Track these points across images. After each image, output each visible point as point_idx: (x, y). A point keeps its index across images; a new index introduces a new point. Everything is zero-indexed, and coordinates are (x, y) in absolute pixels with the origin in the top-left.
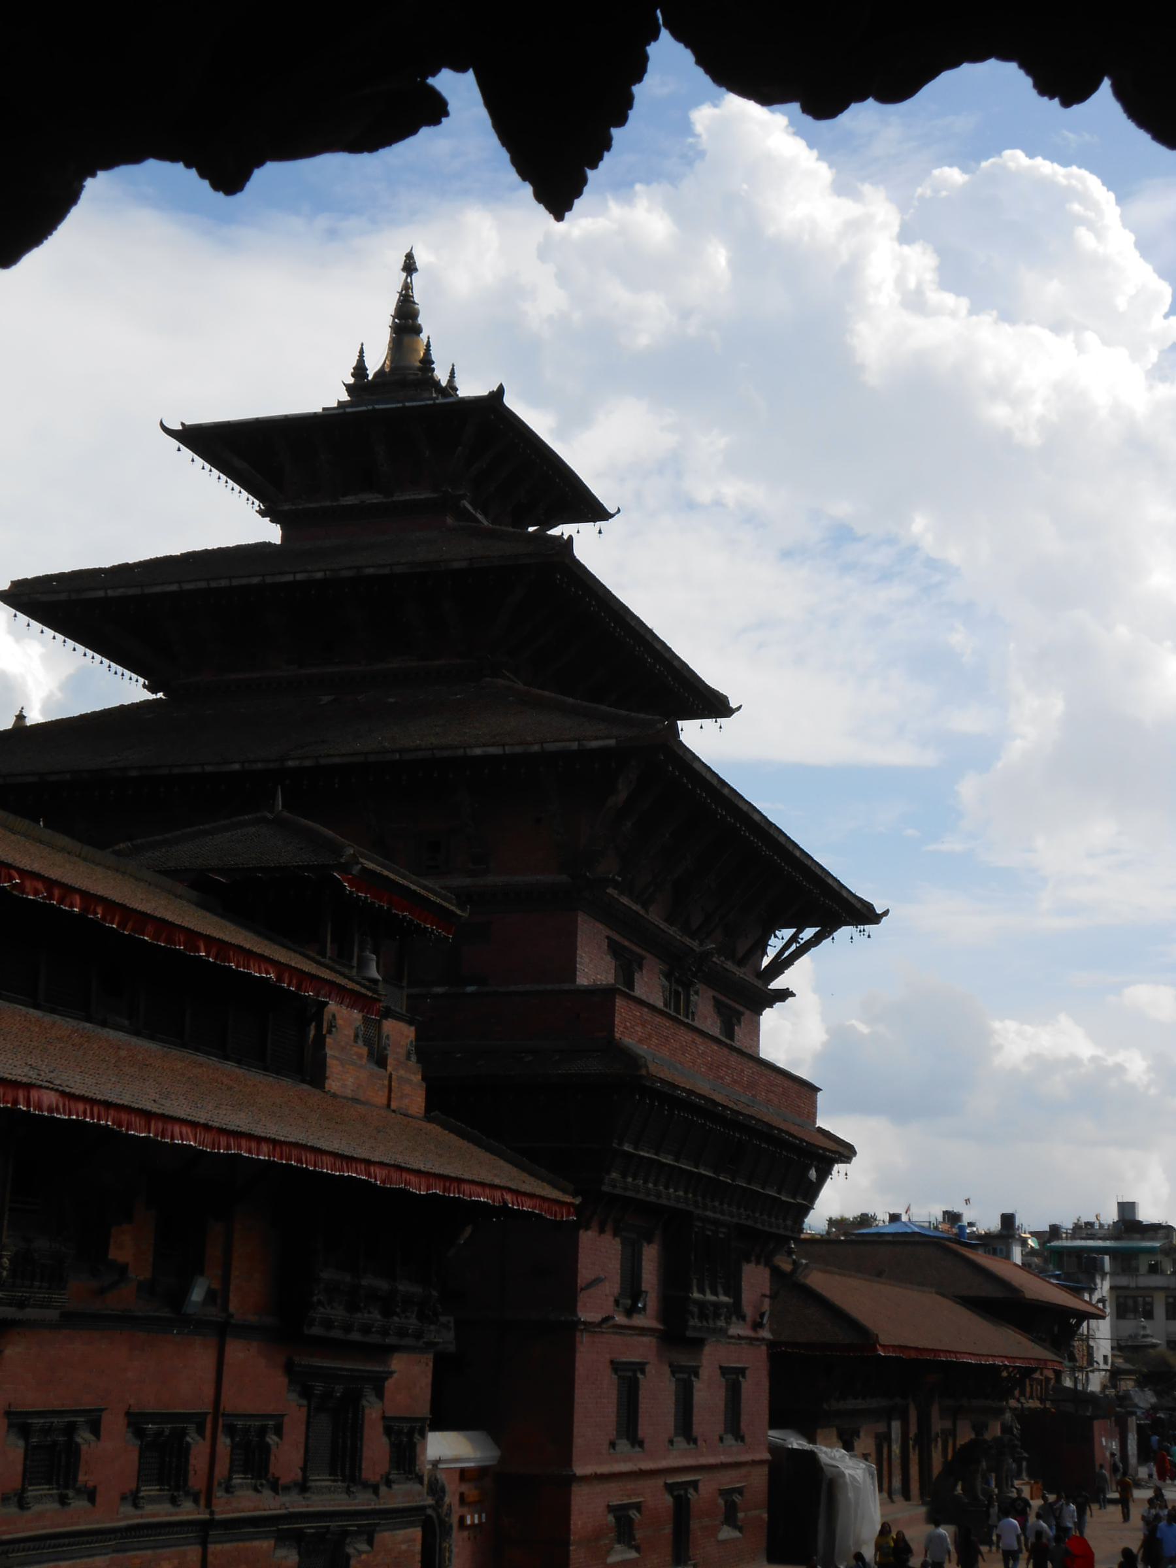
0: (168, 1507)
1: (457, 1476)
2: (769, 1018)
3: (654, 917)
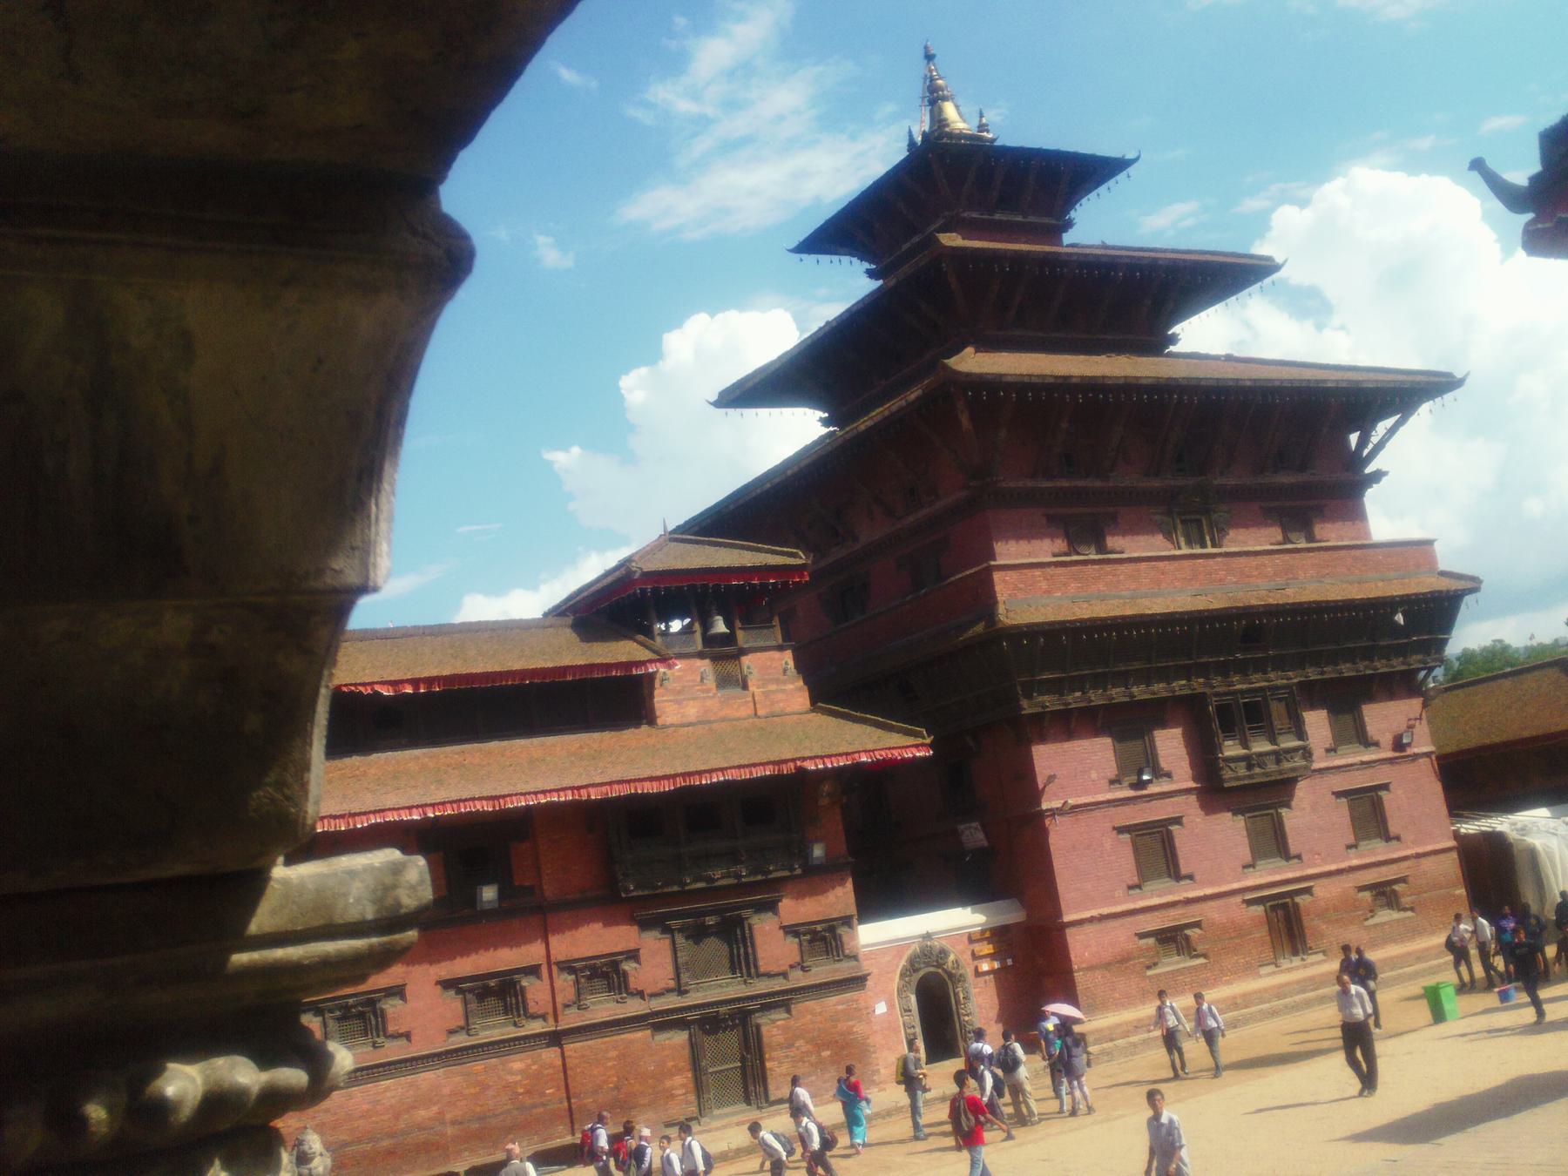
0: (513, 1028)
1: (966, 940)
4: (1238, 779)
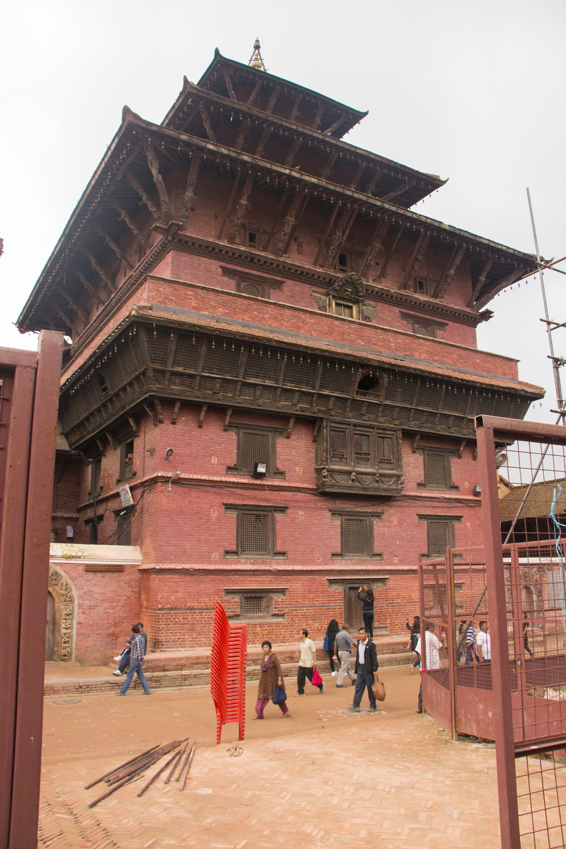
2: (482, 328)
3: (294, 259)
4: (339, 487)
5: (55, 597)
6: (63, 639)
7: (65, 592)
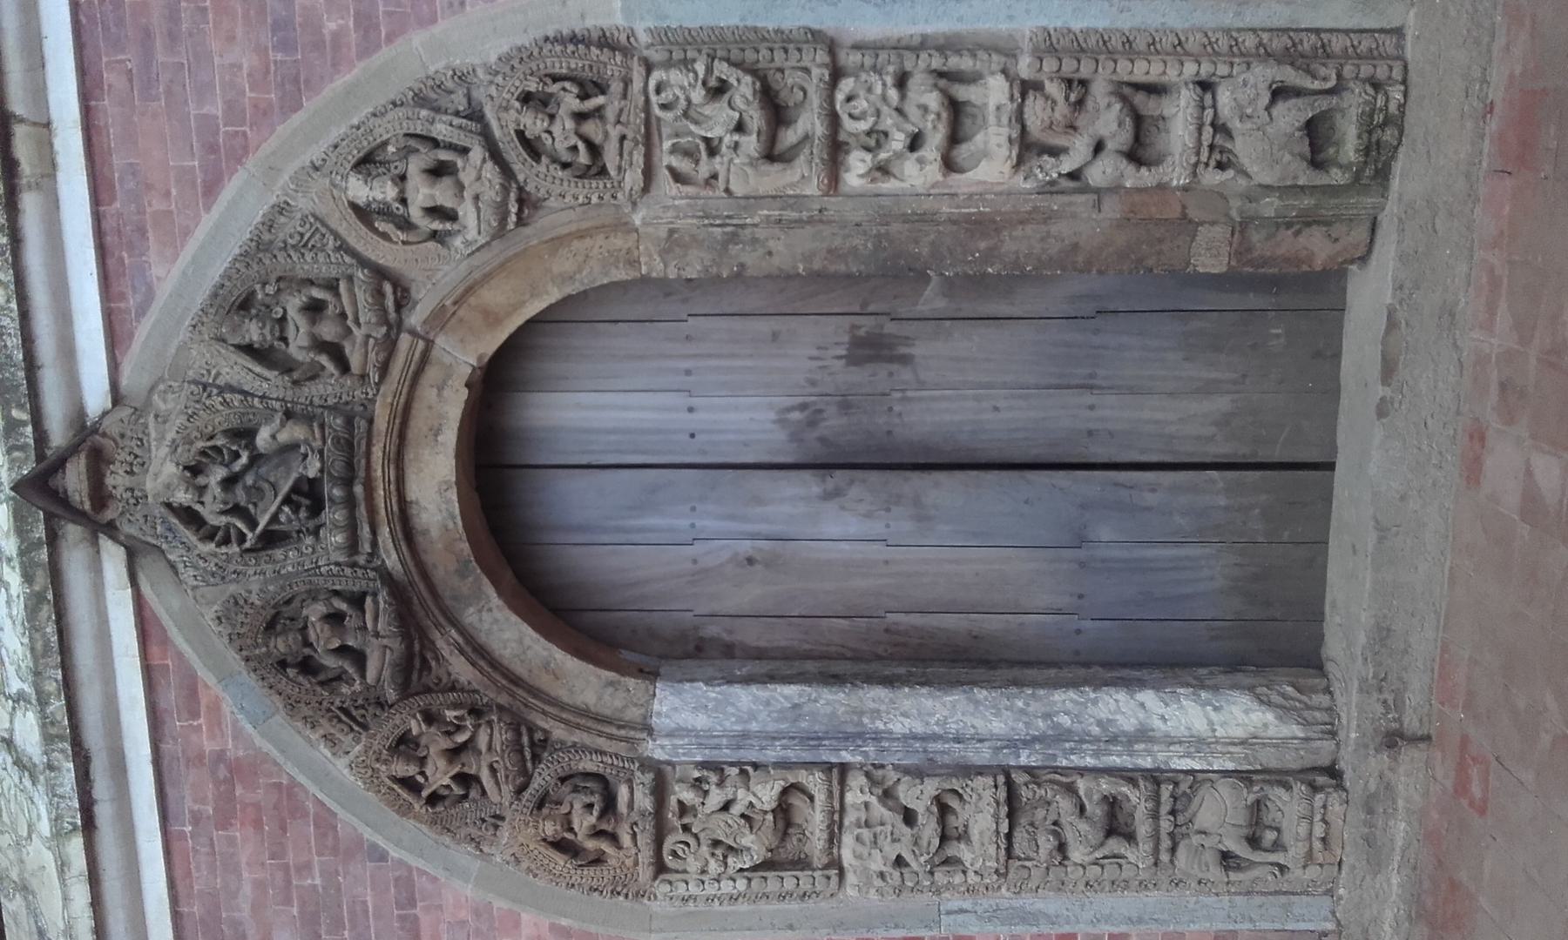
5: (554, 295)
6: (1099, 174)
7: (476, 169)
